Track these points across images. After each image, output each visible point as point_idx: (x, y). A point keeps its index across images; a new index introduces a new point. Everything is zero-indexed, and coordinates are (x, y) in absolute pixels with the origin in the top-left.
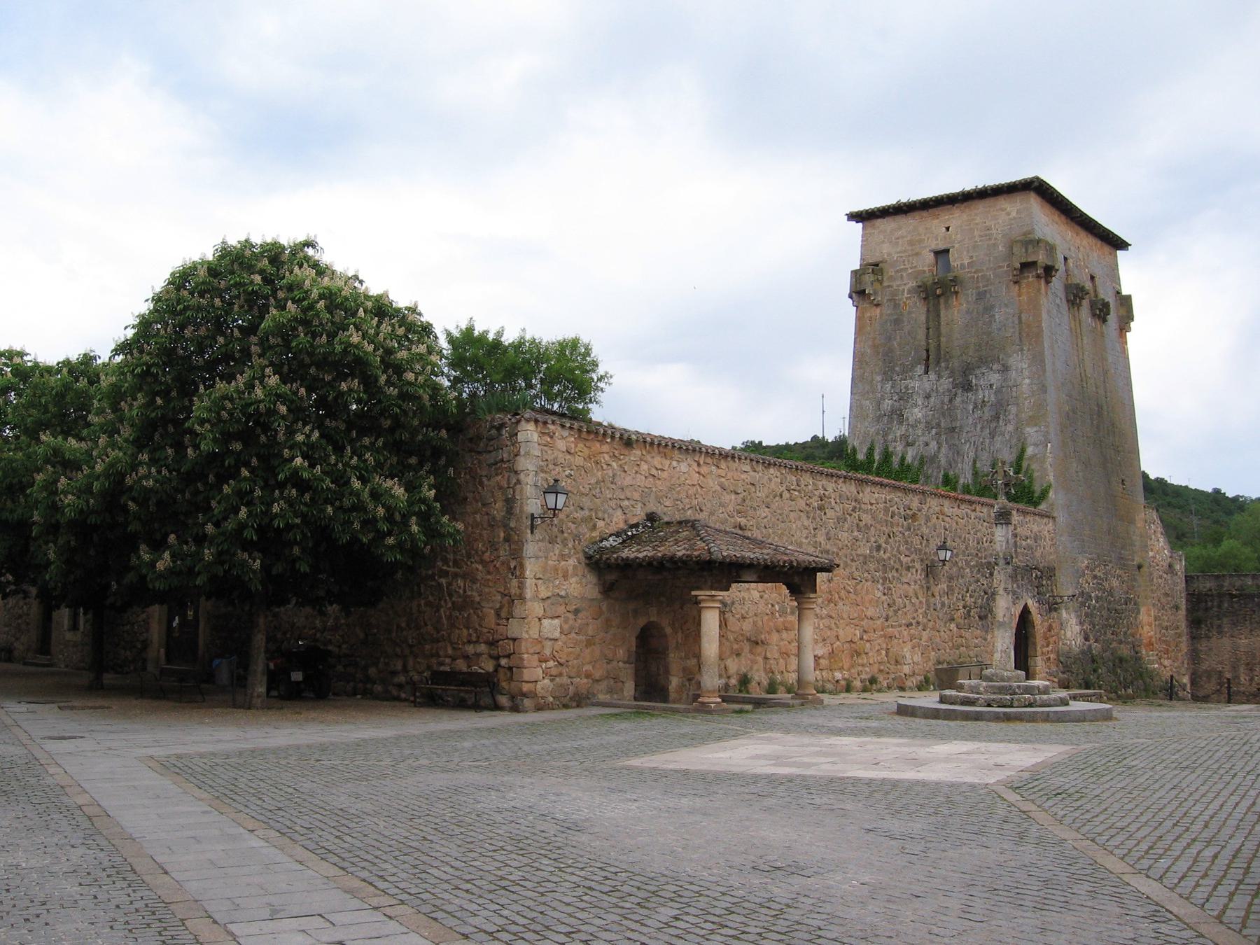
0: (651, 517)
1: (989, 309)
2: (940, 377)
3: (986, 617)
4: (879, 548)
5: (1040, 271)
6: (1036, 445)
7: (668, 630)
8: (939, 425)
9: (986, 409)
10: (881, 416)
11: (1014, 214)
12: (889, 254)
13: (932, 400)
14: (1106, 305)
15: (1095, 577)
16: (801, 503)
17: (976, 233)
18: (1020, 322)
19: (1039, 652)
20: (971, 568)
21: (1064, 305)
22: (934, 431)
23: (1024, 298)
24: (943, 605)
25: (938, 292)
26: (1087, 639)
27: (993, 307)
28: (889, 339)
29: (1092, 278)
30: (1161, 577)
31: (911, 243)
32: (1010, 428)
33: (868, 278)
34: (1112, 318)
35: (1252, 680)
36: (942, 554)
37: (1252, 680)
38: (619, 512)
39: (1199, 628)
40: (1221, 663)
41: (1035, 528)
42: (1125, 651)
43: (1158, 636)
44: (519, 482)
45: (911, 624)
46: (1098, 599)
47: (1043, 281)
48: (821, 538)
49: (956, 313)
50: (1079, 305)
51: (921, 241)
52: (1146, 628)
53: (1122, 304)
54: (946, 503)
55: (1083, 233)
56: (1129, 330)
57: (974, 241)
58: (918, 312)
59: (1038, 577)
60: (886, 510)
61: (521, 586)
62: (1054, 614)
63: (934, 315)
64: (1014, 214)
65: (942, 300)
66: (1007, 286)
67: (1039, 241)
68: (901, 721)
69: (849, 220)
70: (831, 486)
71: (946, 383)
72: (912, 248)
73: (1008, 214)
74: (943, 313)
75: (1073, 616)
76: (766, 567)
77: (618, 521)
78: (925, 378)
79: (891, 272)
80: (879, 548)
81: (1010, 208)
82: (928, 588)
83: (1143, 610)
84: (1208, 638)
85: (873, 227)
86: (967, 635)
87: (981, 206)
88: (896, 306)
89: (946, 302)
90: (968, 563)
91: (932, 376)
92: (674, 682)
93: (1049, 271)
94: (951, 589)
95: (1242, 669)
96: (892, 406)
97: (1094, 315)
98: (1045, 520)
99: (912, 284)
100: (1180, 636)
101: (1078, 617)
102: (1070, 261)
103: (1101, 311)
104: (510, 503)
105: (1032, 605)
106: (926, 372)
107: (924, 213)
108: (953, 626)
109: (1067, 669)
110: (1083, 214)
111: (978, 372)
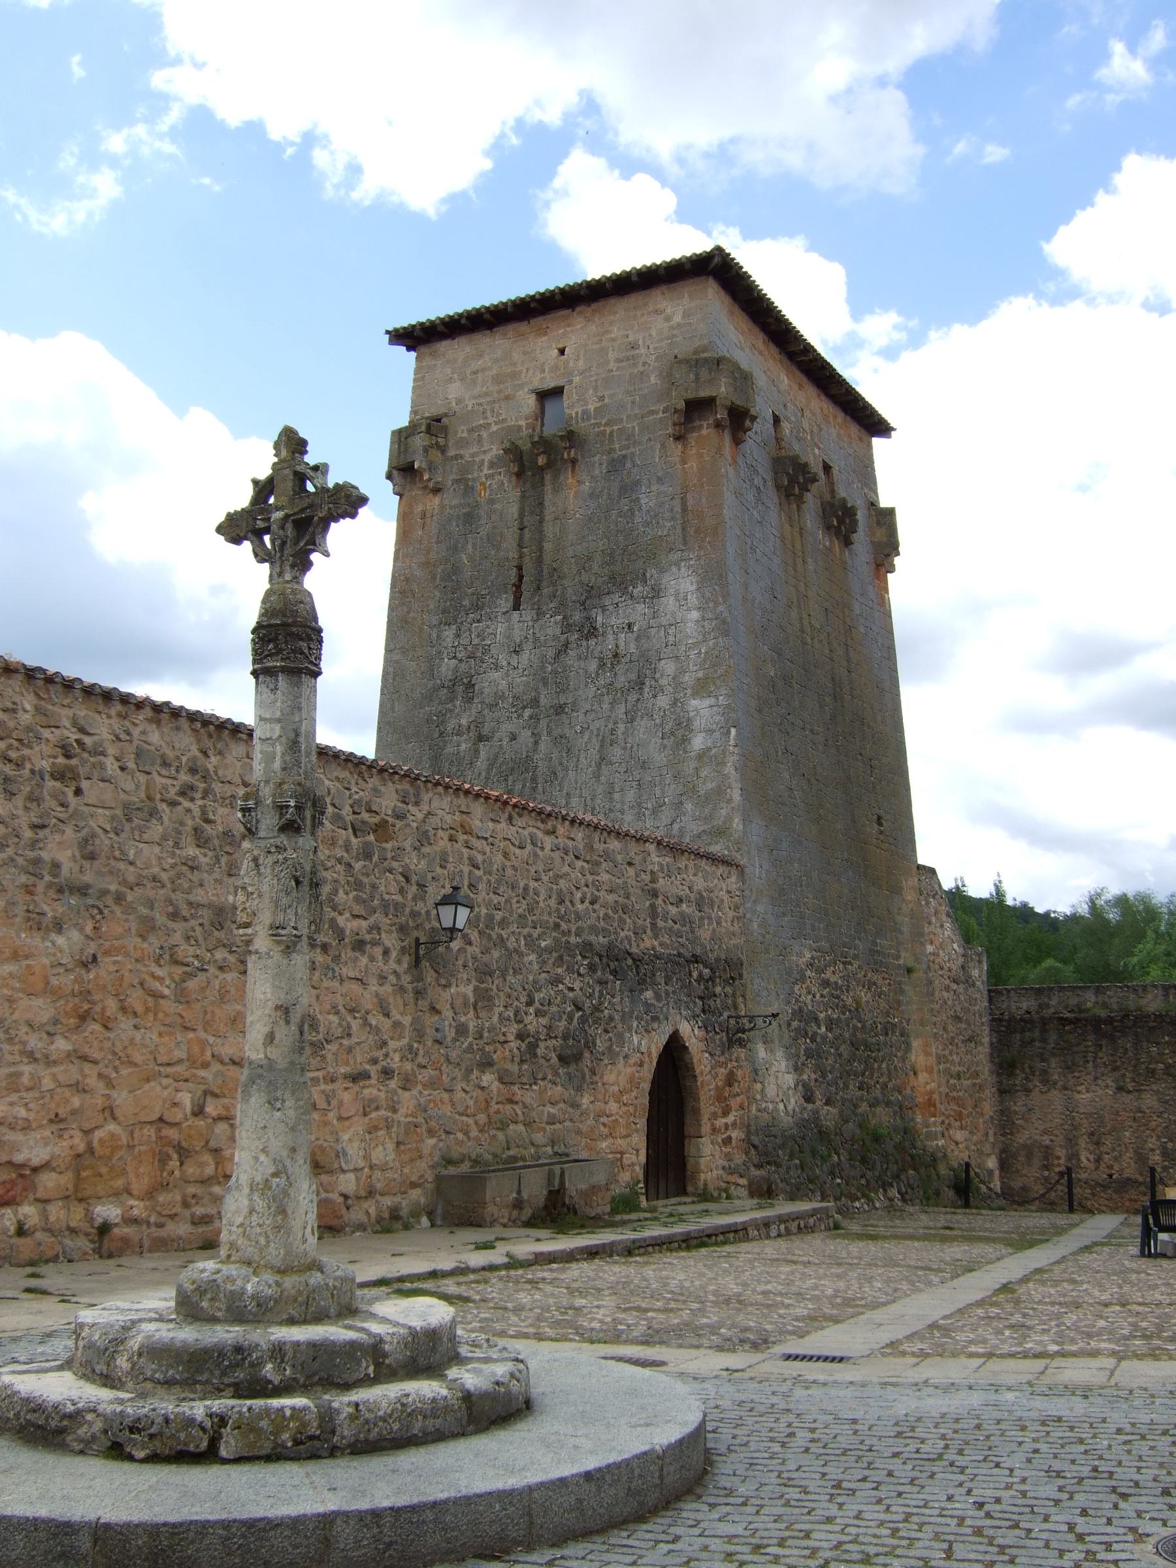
1: (628, 489)
2: (540, 614)
3: (578, 1058)
5: (722, 414)
6: (710, 732)
8: (535, 702)
9: (620, 669)
10: (436, 689)
11: (678, 319)
12: (459, 401)
13: (525, 655)
15: (826, 983)
17: (612, 355)
18: (684, 509)
19: (706, 1128)
20: (541, 952)
21: (771, 496)
22: (527, 713)
23: (692, 465)
24: (462, 1030)
25: (541, 461)
26: (809, 1099)
27: (638, 483)
28: (455, 549)
30: (947, 989)
31: (498, 379)
32: (663, 701)
33: (419, 441)
34: (861, 538)
35: (1098, 1160)
36: (446, 913)
37: (1098, 1160)
39: (1011, 1075)
40: (1045, 1132)
41: (700, 884)
42: (882, 1118)
43: (944, 1089)
45: (365, 1076)
46: (830, 1024)
47: (727, 437)
49: (573, 497)
50: (800, 500)
52: (923, 1076)
53: (879, 524)
54: (478, 808)
55: (811, 391)
56: (892, 569)
58: (502, 495)
63: (533, 506)
64: (678, 319)
65: (548, 477)
66: (663, 446)
67: (719, 361)
69: (391, 342)
71: (552, 626)
72: (499, 387)
73: (668, 319)
74: (548, 497)
75: (780, 1054)
78: (516, 614)
79: (462, 432)
82: (419, 994)
83: (916, 1044)
84: (1028, 1091)
85: (434, 355)
86: (529, 1096)
88: (468, 490)
89: (556, 477)
90: (531, 943)
91: (528, 614)
94: (483, 999)
95: (1083, 1142)
96: (456, 670)
97: (828, 527)
98: (721, 869)
100: (981, 1088)
105: (690, 1032)
106: (516, 607)
107: (523, 327)
108: (488, 1078)
109: (766, 1158)
110: (809, 349)
111: (607, 601)
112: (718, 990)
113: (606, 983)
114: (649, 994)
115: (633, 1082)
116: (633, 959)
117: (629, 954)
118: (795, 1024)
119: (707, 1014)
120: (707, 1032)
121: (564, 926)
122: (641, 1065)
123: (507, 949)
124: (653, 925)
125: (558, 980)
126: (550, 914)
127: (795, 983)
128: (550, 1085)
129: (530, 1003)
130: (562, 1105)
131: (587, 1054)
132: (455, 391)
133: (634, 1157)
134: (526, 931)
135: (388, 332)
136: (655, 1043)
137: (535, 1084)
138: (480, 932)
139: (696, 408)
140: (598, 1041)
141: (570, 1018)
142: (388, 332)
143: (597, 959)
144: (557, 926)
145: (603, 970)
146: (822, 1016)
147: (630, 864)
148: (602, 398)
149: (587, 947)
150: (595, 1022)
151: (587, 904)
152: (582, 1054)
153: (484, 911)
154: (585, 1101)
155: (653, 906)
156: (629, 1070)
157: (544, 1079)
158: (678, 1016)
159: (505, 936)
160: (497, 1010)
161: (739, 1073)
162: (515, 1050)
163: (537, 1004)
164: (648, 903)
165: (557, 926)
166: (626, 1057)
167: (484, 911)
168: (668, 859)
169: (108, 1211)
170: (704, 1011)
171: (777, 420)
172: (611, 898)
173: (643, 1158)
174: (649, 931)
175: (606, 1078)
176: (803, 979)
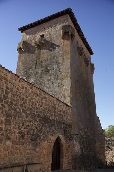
3: (35, 140)
15: (85, 132)
19: (64, 156)
20: (27, 114)
26: (82, 151)
41: (64, 109)
52: (97, 148)
62: (70, 141)
101: (79, 143)
105: (62, 137)
106: (36, 68)
112: (67, 129)
113: (43, 124)
114: (53, 128)
115: (49, 146)
116: (50, 120)
117: (49, 119)
118: (80, 138)
119: (65, 134)
120: (65, 137)
121: (33, 109)
122: (51, 142)
123: (16, 111)
124: (55, 114)
125: (31, 121)
126: (30, 106)
127: (80, 131)
128: (28, 145)
129: (23, 125)
130: (31, 150)
131: (38, 139)
133: (49, 162)
134: (23, 108)
135: (18, 29)
136: (54, 138)
137: (24, 145)
138: (8, 105)
140: (41, 136)
141: (34, 131)
142: (18, 29)
143: (41, 118)
144: (31, 109)
145: (43, 121)
146: (84, 137)
147: (50, 101)
148: (50, 35)
149: (39, 115)
150: (40, 132)
151: (40, 106)
152: (37, 139)
153: (10, 100)
154: (37, 150)
155: (55, 111)
156: (48, 143)
157: (26, 144)
158: (59, 134)
159: (16, 108)
160: (12, 126)
161: (71, 146)
162: (18, 136)
163: (25, 126)
164: (54, 110)
165: (31, 109)
166: (48, 140)
167: (10, 100)
168: (58, 103)
170: (64, 133)
172: (46, 107)
173: (51, 162)
174: (54, 116)
175: (43, 145)
176: (82, 130)
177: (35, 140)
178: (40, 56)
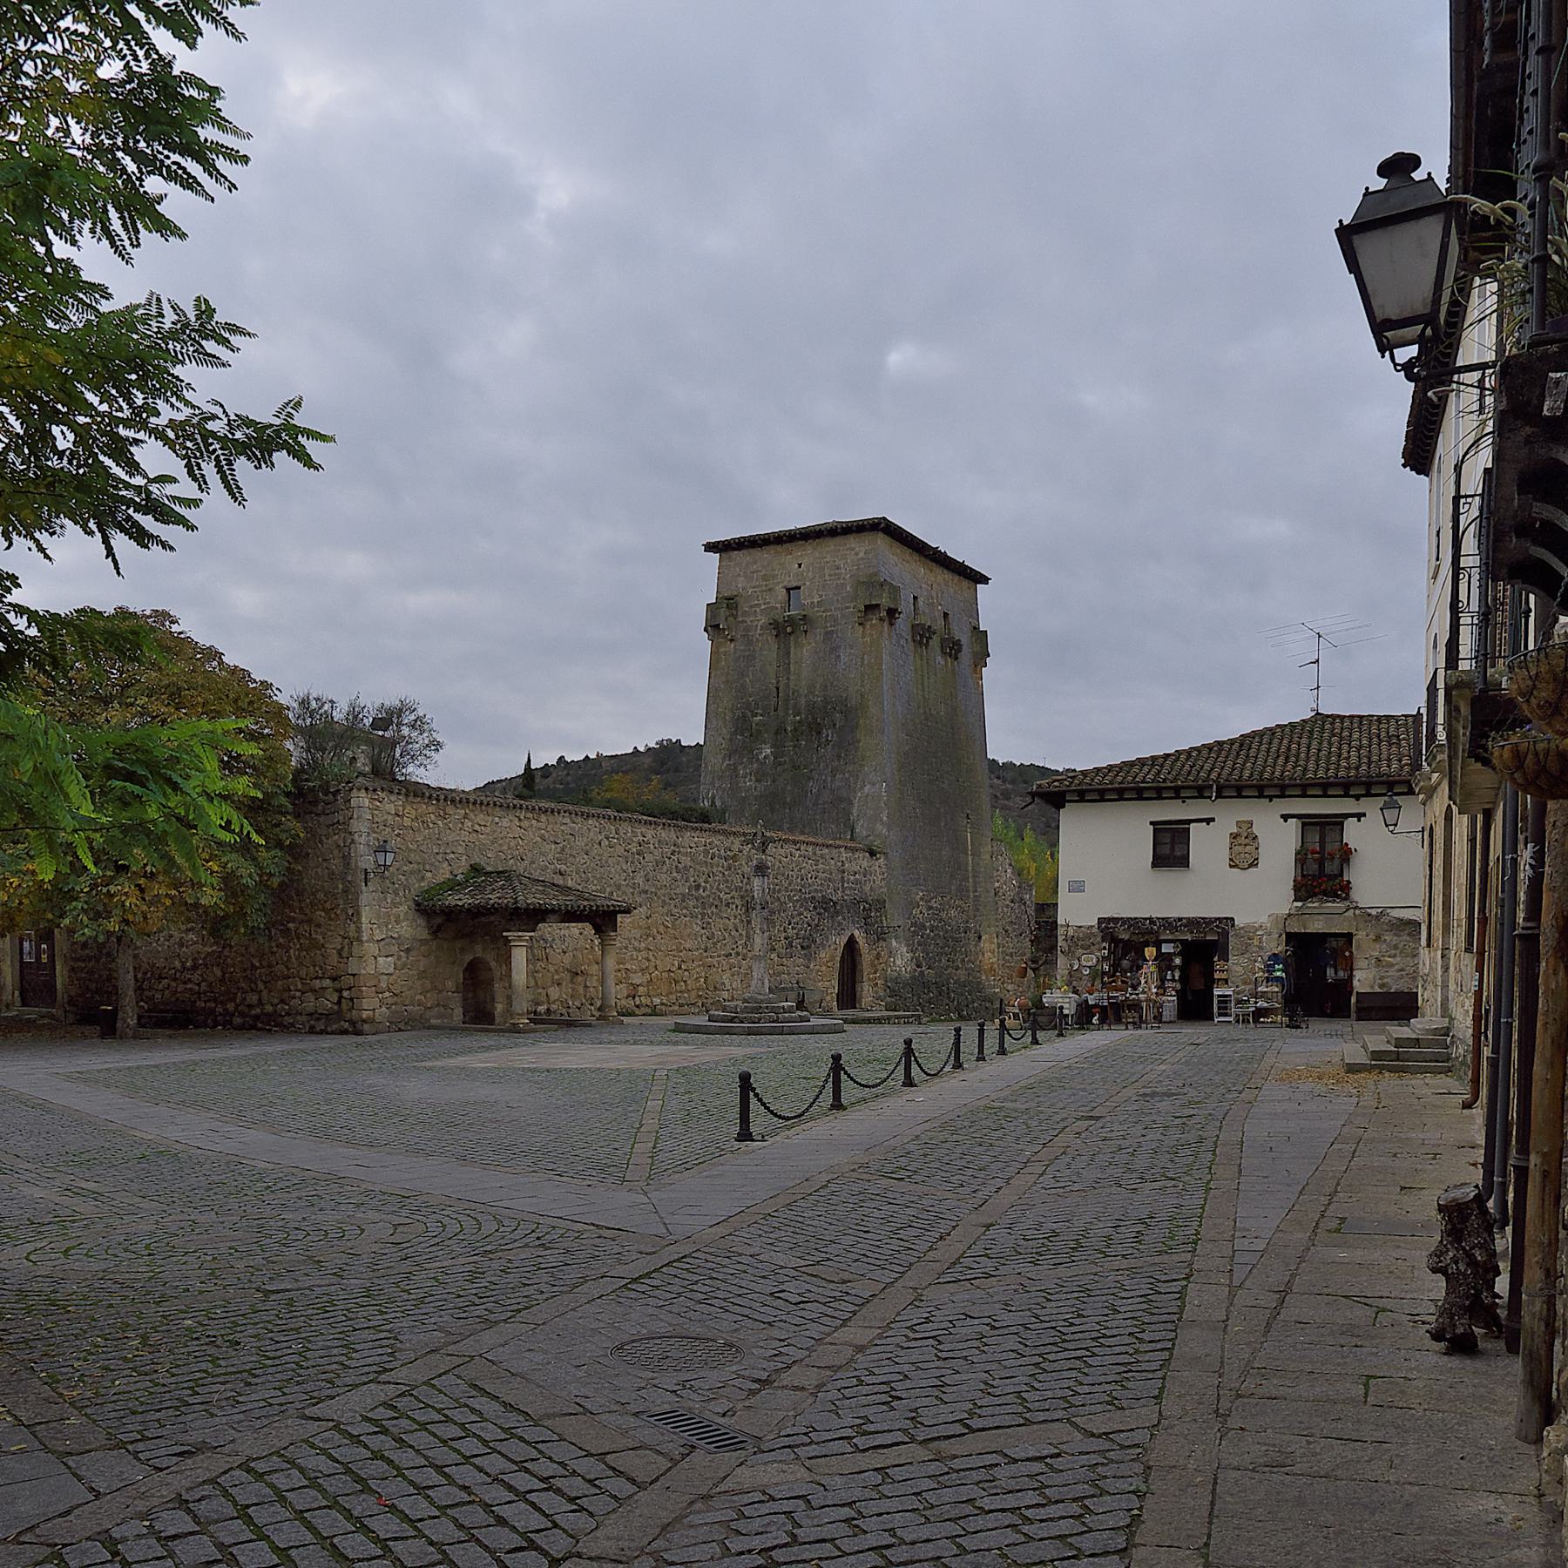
0: (476, 869)
1: (834, 649)
4: (698, 887)
7: (493, 964)
11: (861, 555)
14: (958, 643)
15: (930, 908)
16: (620, 850)
29: (946, 615)
31: (765, 578)
33: (723, 612)
34: (966, 656)
38: (445, 864)
44: (353, 841)
47: (886, 624)
48: (640, 880)
49: (805, 651)
51: (774, 577)
55: (938, 570)
57: (822, 579)
59: (869, 911)
60: (706, 852)
61: (359, 930)
62: (882, 943)
64: (861, 555)
68: (674, 1036)
70: (650, 833)
76: (568, 912)
77: (444, 874)
80: (698, 887)
81: (859, 547)
85: (730, 559)
87: (832, 544)
88: (750, 642)
92: (499, 1008)
93: (892, 613)
97: (943, 653)
99: (763, 620)
102: (921, 600)
103: (952, 649)
104: (346, 858)
107: (779, 548)
109: (893, 993)
115: (832, 958)
132: (741, 583)
139: (870, 608)
169: (657, 1001)
171: (915, 598)
177: (808, 946)
178: (788, 670)
